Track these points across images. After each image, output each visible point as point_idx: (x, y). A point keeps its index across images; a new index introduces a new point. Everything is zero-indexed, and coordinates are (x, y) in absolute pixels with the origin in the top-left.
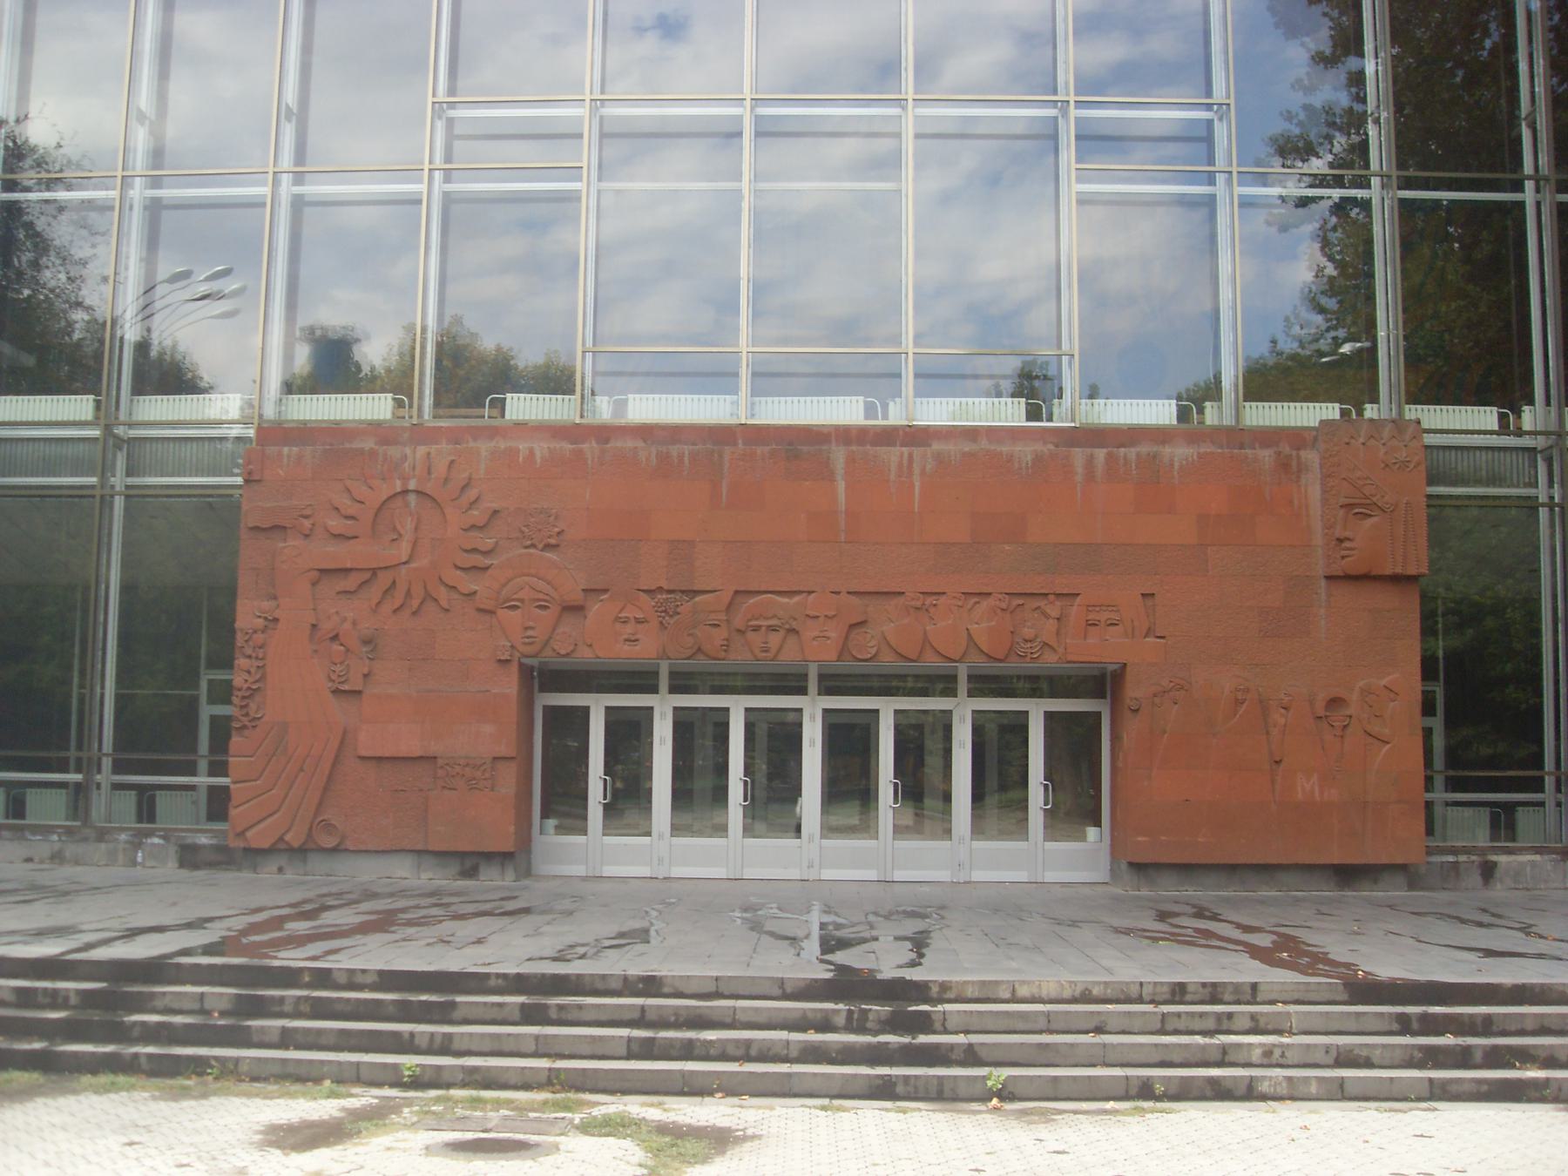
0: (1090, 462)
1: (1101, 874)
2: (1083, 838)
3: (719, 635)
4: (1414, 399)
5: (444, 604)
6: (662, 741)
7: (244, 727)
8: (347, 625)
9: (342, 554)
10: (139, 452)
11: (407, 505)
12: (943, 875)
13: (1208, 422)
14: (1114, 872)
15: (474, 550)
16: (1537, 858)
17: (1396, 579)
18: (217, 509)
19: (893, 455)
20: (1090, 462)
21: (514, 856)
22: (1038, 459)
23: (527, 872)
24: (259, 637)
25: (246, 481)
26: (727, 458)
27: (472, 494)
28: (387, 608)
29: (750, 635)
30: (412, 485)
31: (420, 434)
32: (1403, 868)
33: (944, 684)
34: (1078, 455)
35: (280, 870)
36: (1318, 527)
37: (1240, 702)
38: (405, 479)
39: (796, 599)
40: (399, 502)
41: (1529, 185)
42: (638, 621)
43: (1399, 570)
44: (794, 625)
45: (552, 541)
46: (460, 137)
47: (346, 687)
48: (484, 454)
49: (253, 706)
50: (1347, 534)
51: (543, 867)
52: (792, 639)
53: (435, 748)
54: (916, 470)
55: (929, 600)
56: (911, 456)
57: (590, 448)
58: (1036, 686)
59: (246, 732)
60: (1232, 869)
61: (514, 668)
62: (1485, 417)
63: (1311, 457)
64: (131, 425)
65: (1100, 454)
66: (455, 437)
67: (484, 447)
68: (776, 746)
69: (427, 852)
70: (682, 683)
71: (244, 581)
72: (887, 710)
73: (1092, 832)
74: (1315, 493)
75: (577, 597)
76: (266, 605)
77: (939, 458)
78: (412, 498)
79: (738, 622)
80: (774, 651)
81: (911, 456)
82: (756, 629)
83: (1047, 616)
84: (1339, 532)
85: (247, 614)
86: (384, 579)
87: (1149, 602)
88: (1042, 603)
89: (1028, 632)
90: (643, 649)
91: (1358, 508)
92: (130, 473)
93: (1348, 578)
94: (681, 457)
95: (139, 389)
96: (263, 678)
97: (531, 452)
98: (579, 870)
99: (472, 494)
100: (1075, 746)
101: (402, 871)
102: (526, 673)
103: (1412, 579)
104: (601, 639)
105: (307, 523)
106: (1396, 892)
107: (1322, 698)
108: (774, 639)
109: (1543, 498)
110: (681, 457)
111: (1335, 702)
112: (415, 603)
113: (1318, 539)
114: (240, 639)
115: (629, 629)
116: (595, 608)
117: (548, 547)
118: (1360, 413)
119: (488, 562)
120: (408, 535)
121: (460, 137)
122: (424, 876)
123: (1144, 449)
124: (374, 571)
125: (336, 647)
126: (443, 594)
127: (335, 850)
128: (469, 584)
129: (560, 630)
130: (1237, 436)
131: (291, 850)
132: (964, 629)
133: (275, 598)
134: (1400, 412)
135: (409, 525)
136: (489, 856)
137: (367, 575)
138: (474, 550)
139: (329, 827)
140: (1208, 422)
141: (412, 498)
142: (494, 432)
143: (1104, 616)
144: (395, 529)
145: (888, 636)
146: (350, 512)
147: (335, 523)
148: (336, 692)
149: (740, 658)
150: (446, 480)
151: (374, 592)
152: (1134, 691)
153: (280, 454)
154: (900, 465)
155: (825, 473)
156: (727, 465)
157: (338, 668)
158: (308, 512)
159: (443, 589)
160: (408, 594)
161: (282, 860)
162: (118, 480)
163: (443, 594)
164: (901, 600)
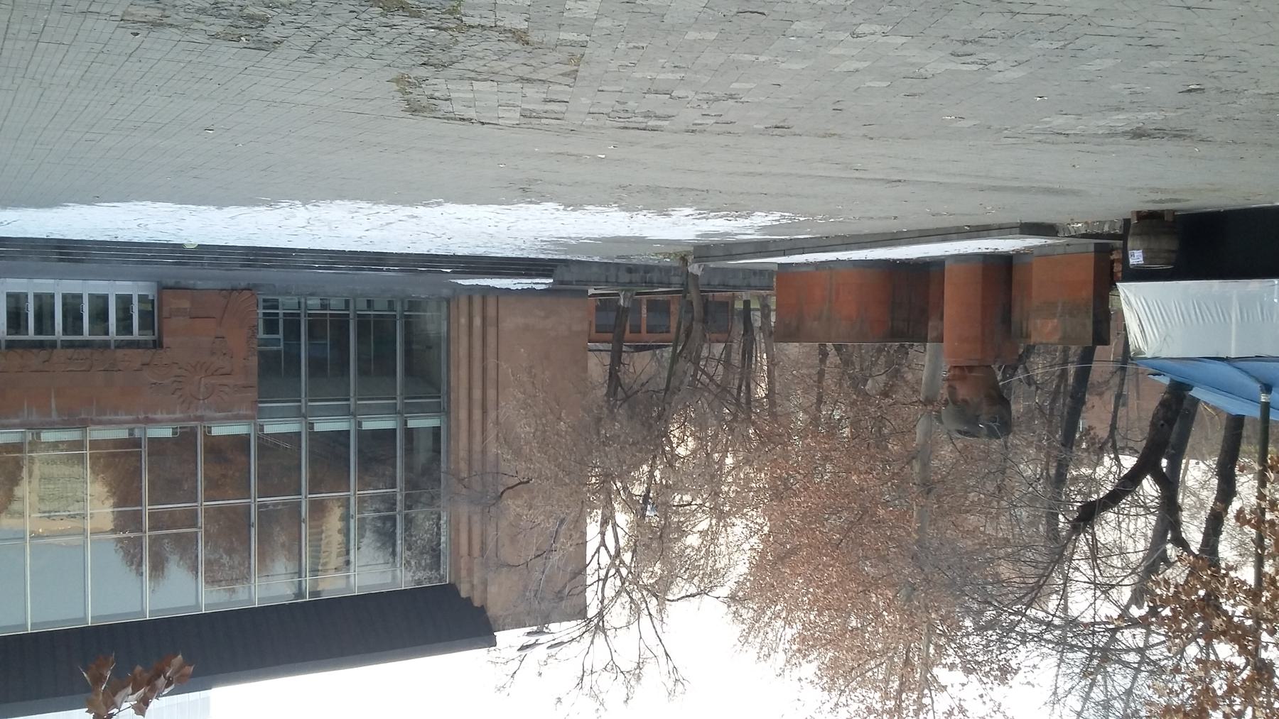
9: (225, 380)
10: (299, 414)
12: (8, 280)
18: (265, 395)
19: (35, 418)
21: (162, 288)
23: (159, 283)
31: (201, 419)
51: (154, 284)
66: (190, 419)
67: (178, 415)
70: (105, 345)
71: (255, 370)
77: (18, 417)
85: (254, 361)
90: (120, 353)
95: (299, 434)
101: (200, 284)
102: (161, 346)
142: (175, 420)
145: (35, 359)
147: (227, 389)
149: (87, 351)
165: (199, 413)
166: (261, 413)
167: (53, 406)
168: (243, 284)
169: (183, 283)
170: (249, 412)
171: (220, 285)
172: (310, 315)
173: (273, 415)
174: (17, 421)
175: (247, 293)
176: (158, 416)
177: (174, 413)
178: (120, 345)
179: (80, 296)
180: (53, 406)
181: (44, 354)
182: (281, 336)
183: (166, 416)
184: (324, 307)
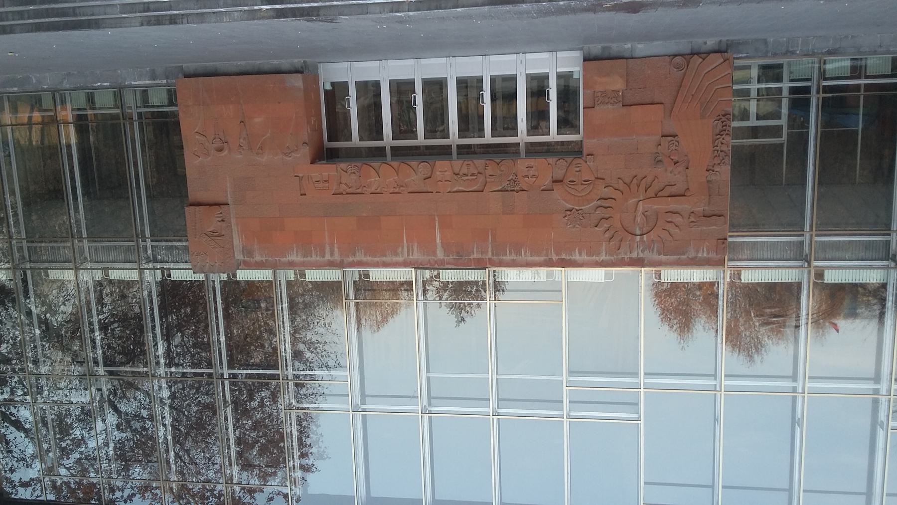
0: (332, 254)
1: (321, 66)
2: (333, 84)
3: (489, 171)
4: (201, 285)
5: (620, 181)
6: (522, 120)
7: (724, 116)
8: (670, 169)
11: (640, 229)
13: (292, 272)
14: (316, 68)
15: (606, 208)
16: (133, 83)
17: (199, 204)
20: (332, 254)
22: (354, 254)
24: (717, 161)
25: (726, 239)
26: (490, 253)
27: (607, 235)
28: (649, 179)
29: (476, 172)
30: (638, 238)
32: (187, 76)
33: (397, 152)
34: (337, 257)
35: (705, 43)
36: (234, 228)
37: (261, 148)
38: (642, 241)
39: (455, 189)
40: (645, 230)
41: (226, 376)
42: (527, 176)
43: (198, 208)
44: (456, 177)
45: (569, 213)
46: (434, 398)
47: (670, 138)
48: (604, 253)
49: (720, 127)
50: (219, 224)
51: (577, 55)
52: (457, 171)
53: (625, 109)
54: (406, 249)
55: (397, 190)
56: (408, 255)
57: (555, 258)
58: (354, 154)
59: (723, 113)
60: (258, 73)
61: (585, 152)
62: (176, 275)
63: (239, 257)
64: (802, 266)
65: (328, 257)
67: (603, 257)
68: (470, 121)
69: (627, 58)
72: (421, 139)
73: (328, 87)
74: (237, 241)
75: (556, 187)
76: (713, 178)
77: (396, 254)
78: (638, 232)
79: (481, 179)
80: (464, 165)
81: (408, 255)
82: (473, 175)
83: (346, 184)
84: (224, 224)
85: (725, 172)
86: (651, 192)
87: (303, 192)
88: (349, 190)
89: (353, 177)
90: (522, 164)
91: (216, 235)
92: (802, 243)
93: (219, 205)
94: (510, 253)
96: (714, 142)
97: (580, 254)
98: (560, 54)
99: (607, 235)
100: (338, 126)
101: (641, 49)
103: (191, 205)
104: (545, 169)
105: (692, 219)
106: (190, 66)
107: (226, 152)
108: (464, 170)
109: (149, 241)
110: (510, 253)
111: (220, 150)
112: (635, 181)
113: (233, 221)
114: (728, 160)
115: (531, 172)
116: (547, 182)
117: (571, 211)
118: (229, 277)
119: (599, 203)
120: (639, 214)
121: (434, 398)
122: (629, 46)
123: (309, 259)
124: (656, 196)
125: (676, 158)
126: (621, 186)
127: (676, 56)
128: (608, 192)
129: (564, 171)
130: (275, 267)
131: (698, 54)
132: (382, 177)
133: (708, 181)
134: (207, 277)
135: (639, 219)
136: (597, 59)
137: (660, 194)
138: (606, 208)
139: (678, 67)
140: (292, 272)
141: (638, 232)
143: (321, 185)
144: (646, 217)
145: (415, 173)
146: (670, 225)
147: (678, 219)
148: (674, 136)
149: (480, 163)
150: (621, 241)
151: (656, 187)
152: (305, 152)
153: (708, 253)
154: (413, 250)
155: (446, 248)
156: (490, 250)
157: (674, 147)
158: (692, 224)
159: (621, 189)
160: (638, 186)
161: (704, 48)
162: (807, 239)
163: (621, 186)
164: (410, 190)
165: (634, 255)
166: (735, 251)
167: (438, 241)
168: (711, 43)
169: (615, 48)
170: (713, 255)
171: (671, 47)
172: (827, 89)
173: (756, 255)
174: (400, 259)
175: (717, 59)
176: (576, 257)
177: (599, 254)
178: (534, 150)
179: (411, 83)
180: (438, 241)
181: (423, 168)
182: (783, 122)
183: (585, 257)
184: (857, 71)
